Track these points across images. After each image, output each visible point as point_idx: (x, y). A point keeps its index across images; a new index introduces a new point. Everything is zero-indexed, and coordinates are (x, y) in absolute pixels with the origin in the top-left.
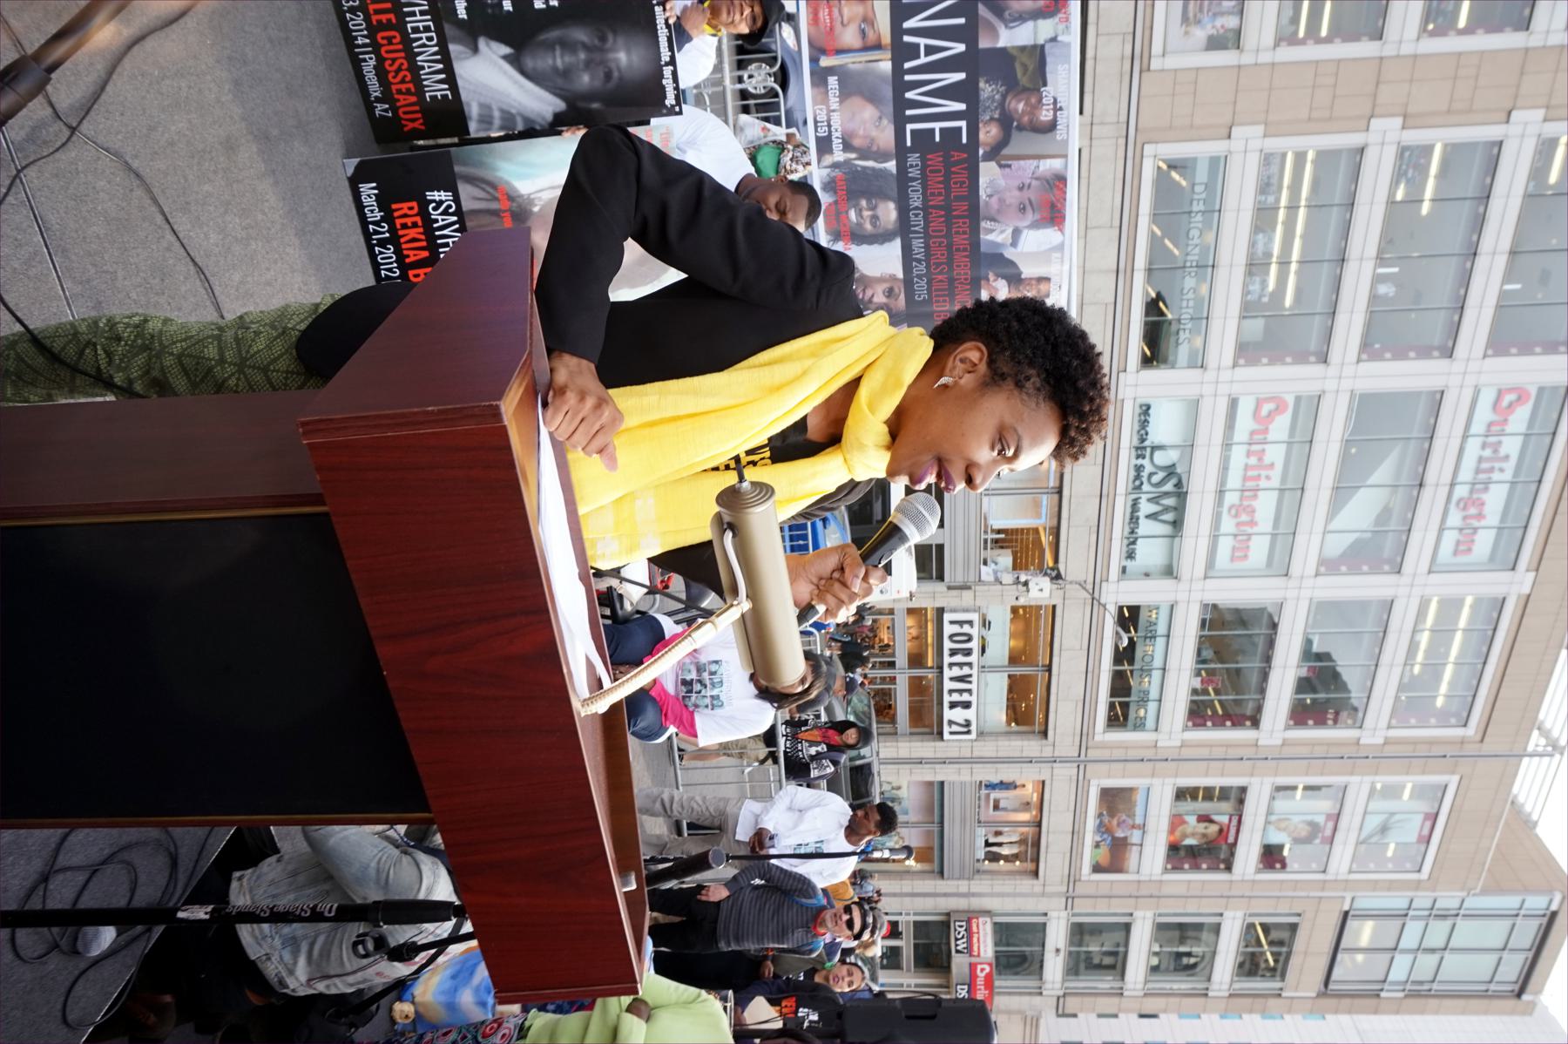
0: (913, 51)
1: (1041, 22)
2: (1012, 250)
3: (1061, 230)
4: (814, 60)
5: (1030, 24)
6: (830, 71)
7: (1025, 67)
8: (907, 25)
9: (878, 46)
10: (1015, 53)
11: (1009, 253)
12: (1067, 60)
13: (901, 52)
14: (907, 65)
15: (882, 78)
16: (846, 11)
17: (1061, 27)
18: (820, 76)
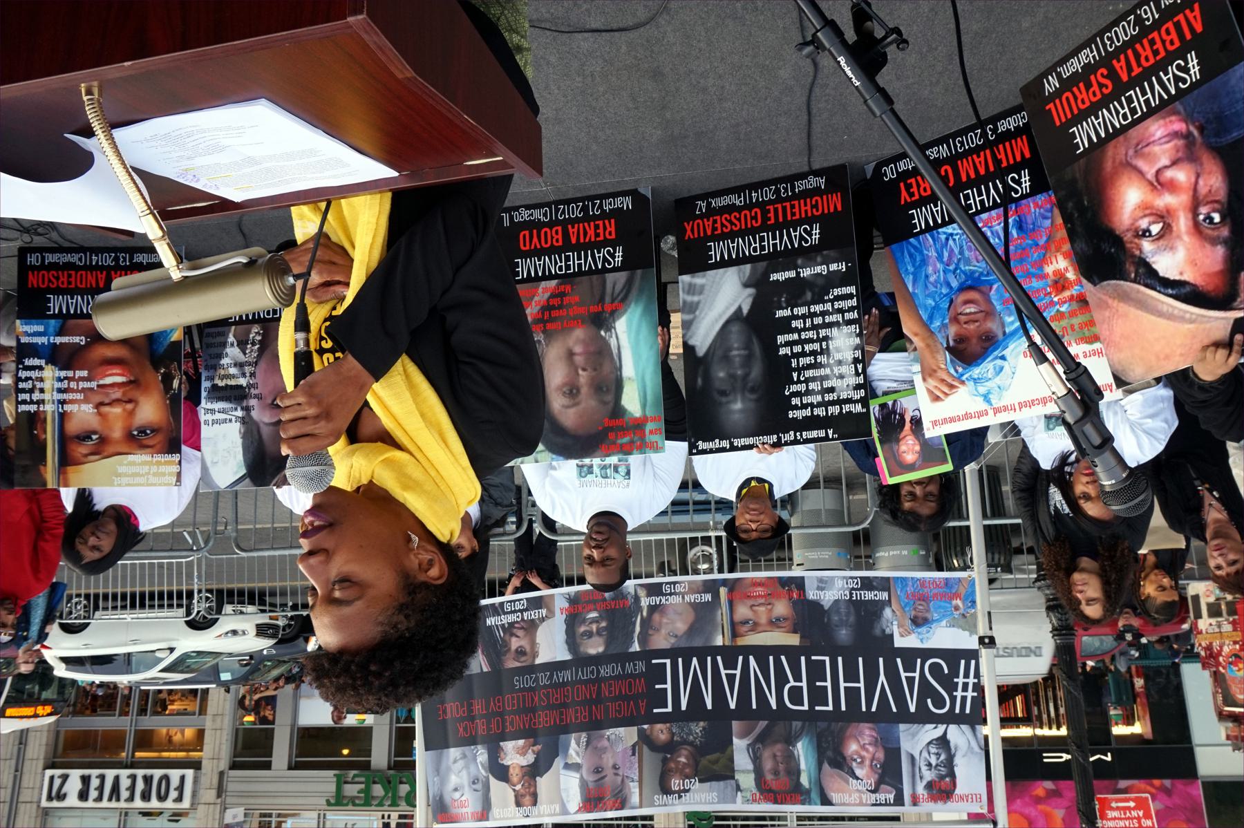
0: (730, 665)
1: (752, 776)
2: (562, 765)
3: (579, 809)
4: (724, 582)
5: (751, 767)
6: (716, 596)
7: (717, 761)
8: (751, 658)
9: (735, 635)
10: (728, 752)
11: (558, 763)
12: (722, 800)
13: (730, 654)
14: (719, 658)
15: (711, 636)
16: (762, 609)
17: (749, 795)
18: (712, 587)
